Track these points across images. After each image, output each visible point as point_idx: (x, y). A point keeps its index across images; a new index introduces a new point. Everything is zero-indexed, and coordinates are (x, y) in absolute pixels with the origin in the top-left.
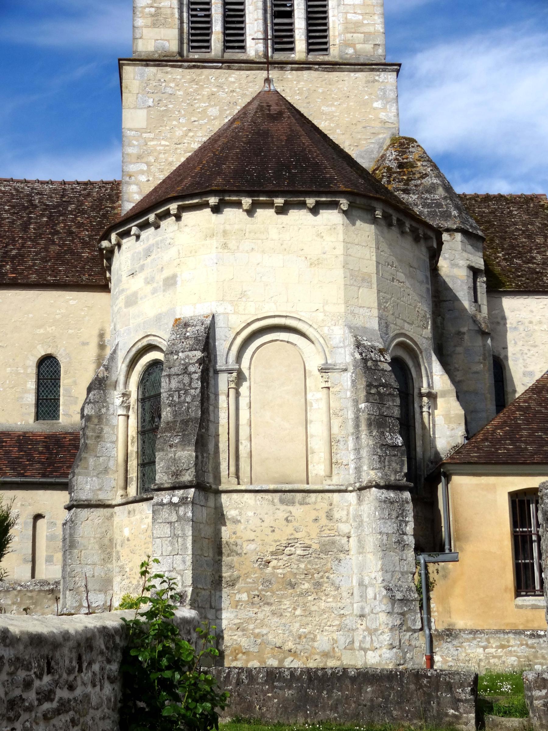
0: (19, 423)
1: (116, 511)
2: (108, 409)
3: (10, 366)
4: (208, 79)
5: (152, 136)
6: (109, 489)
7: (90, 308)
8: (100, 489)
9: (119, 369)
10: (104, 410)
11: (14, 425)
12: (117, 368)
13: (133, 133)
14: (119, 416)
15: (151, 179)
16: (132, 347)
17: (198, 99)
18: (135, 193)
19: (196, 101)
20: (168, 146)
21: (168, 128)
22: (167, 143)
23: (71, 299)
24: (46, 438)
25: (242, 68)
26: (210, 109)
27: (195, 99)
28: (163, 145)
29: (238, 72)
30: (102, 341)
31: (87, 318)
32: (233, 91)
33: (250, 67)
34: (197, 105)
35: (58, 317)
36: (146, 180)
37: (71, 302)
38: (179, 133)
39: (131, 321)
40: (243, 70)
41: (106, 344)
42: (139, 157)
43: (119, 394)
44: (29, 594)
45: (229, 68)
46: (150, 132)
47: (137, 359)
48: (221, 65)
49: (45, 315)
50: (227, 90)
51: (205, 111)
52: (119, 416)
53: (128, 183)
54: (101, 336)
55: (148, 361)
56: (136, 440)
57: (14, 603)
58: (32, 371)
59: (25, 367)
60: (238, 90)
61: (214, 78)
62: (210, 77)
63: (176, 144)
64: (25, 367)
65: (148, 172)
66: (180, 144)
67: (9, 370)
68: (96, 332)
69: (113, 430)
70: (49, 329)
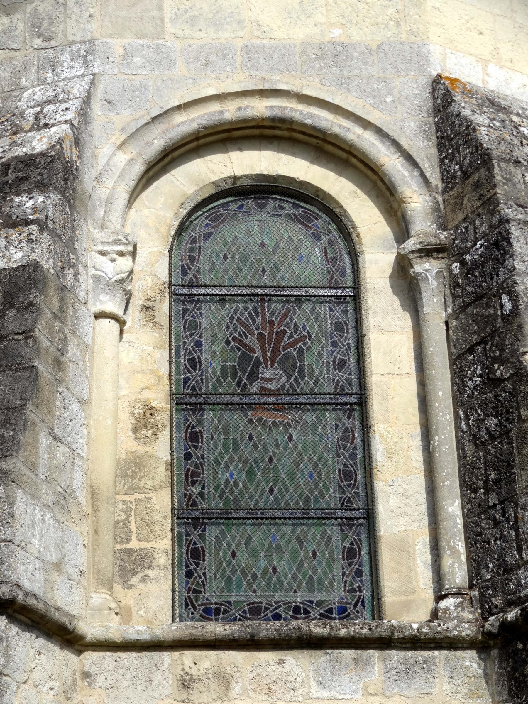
1: (93, 670)
2: (76, 275)
6: (74, 573)
8: (58, 566)
9: (102, 161)
10: (69, 274)
12: (95, 156)
14: (99, 316)
16: (179, 108)
39: (169, 28)
43: (117, 242)
47: (176, 154)
52: (99, 316)
55: (238, 173)
56: (163, 418)
69: (84, 356)
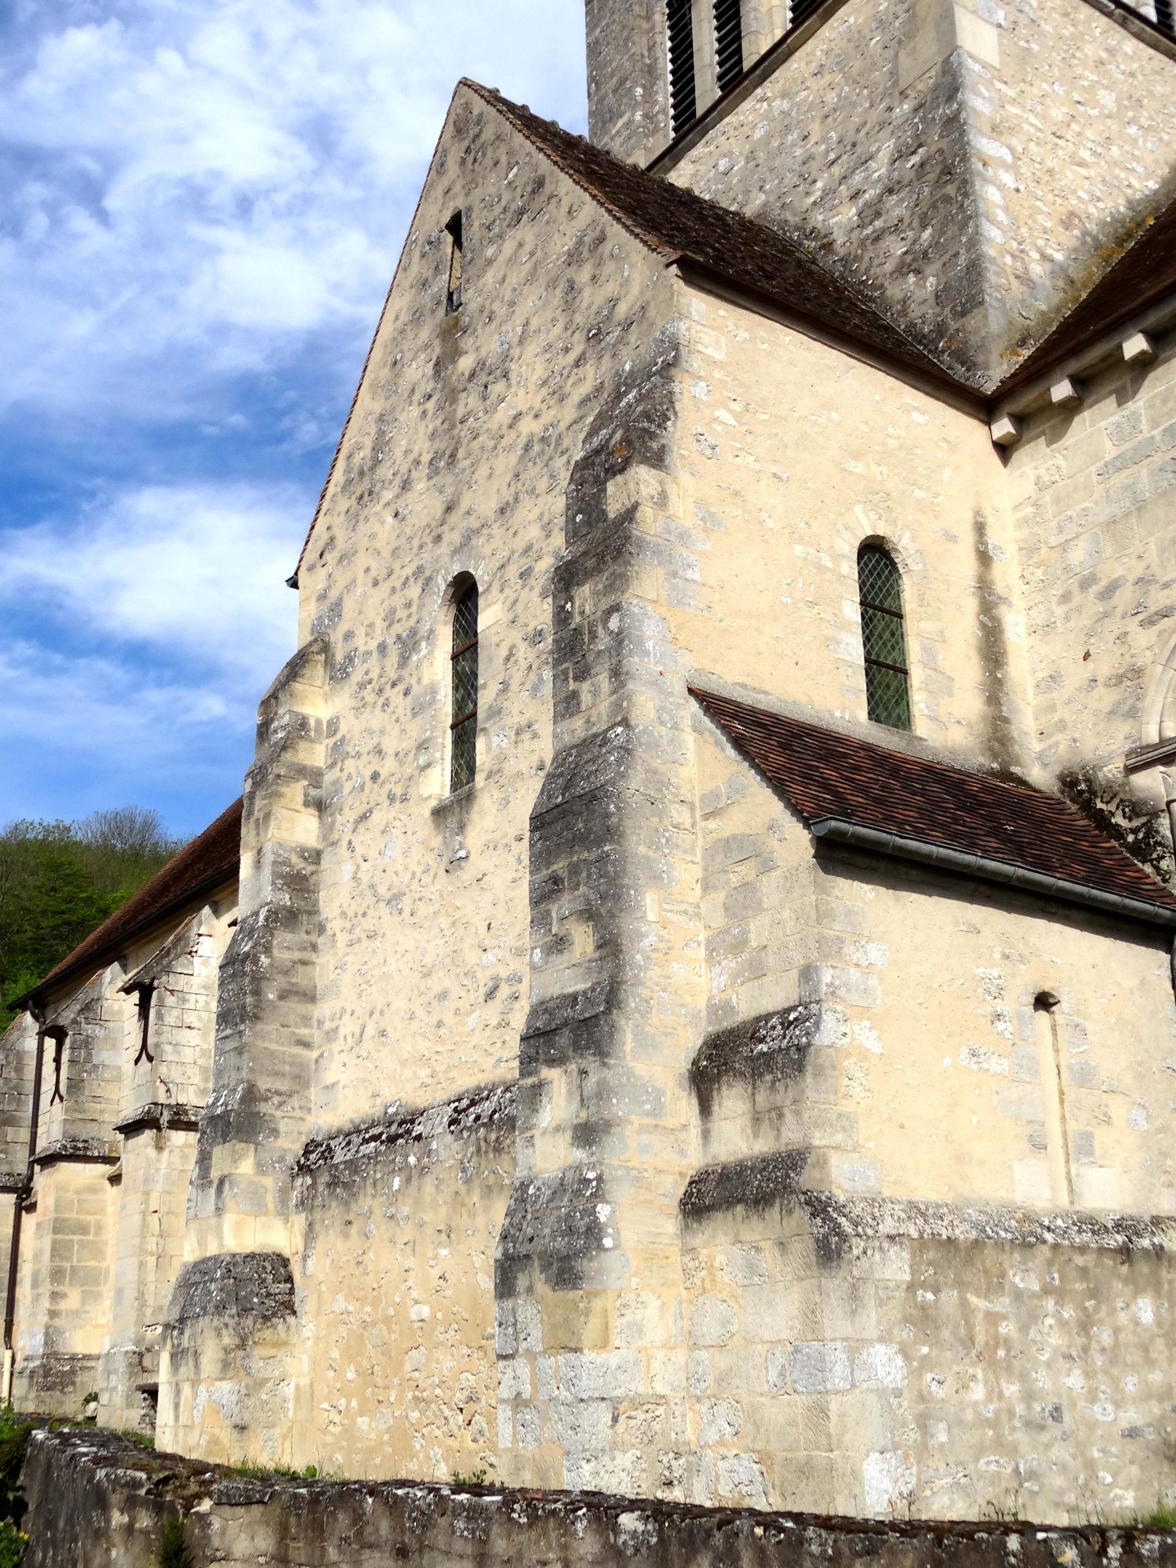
0: (838, 714)
3: (801, 540)
4: (1090, 28)
5: (1012, 93)
7: (953, 447)
11: (827, 716)
13: (977, 67)
15: (1022, 188)
17: (1079, 59)
18: (998, 206)
19: (1076, 62)
20: (1039, 130)
21: (1035, 91)
22: (1040, 125)
23: (916, 408)
24: (924, 770)
25: (1144, 35)
26: (1102, 92)
27: (1073, 56)
28: (1031, 124)
29: (1135, 41)
30: (982, 543)
31: (947, 472)
32: (1132, 75)
33: (1159, 40)
34: (1079, 71)
35: (892, 443)
36: (1013, 186)
37: (916, 417)
38: (1058, 113)
40: (1143, 41)
41: (991, 554)
42: (996, 130)
44: (1079, 1260)
45: (1123, 24)
46: (1006, 83)
48: (1112, 6)
49: (864, 428)
50: (1123, 67)
51: (1092, 88)
53: (985, 180)
54: (980, 529)
57: (1046, 1291)
58: (850, 569)
59: (837, 557)
60: (1140, 78)
61: (1098, 30)
62: (1094, 25)
63: (1053, 134)
64: (837, 557)
65: (1014, 168)
66: (1060, 137)
67: (799, 549)
68: (968, 519)
70: (875, 469)
